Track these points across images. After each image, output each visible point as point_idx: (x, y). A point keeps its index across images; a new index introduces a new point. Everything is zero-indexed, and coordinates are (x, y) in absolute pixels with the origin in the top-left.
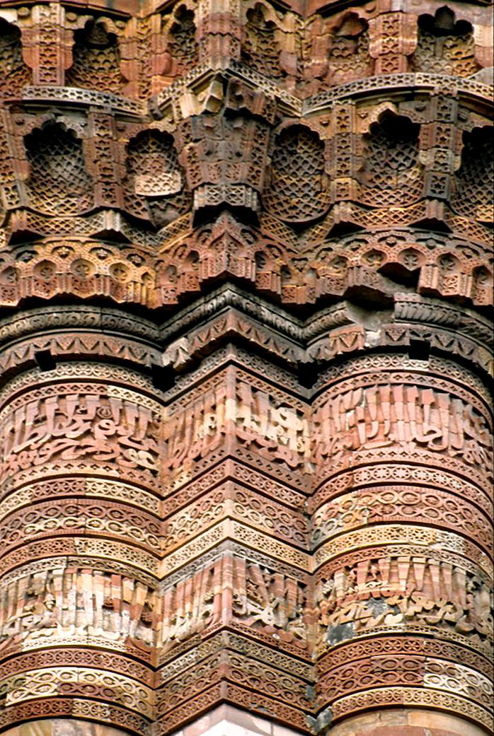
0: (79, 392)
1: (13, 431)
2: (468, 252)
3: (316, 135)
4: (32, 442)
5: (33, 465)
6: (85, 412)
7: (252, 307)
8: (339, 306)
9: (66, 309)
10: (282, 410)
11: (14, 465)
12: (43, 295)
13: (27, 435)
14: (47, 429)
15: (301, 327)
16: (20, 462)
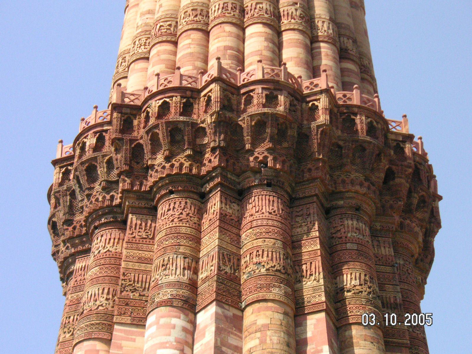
0: (180, 201)
1: (162, 213)
2: (280, 155)
3: (241, 126)
4: (166, 216)
5: (166, 223)
6: (181, 207)
7: (225, 174)
8: (248, 172)
9: (177, 176)
10: (233, 204)
11: (162, 224)
12: (171, 173)
13: (165, 214)
14: (171, 212)
15: (238, 179)
16: (163, 222)
